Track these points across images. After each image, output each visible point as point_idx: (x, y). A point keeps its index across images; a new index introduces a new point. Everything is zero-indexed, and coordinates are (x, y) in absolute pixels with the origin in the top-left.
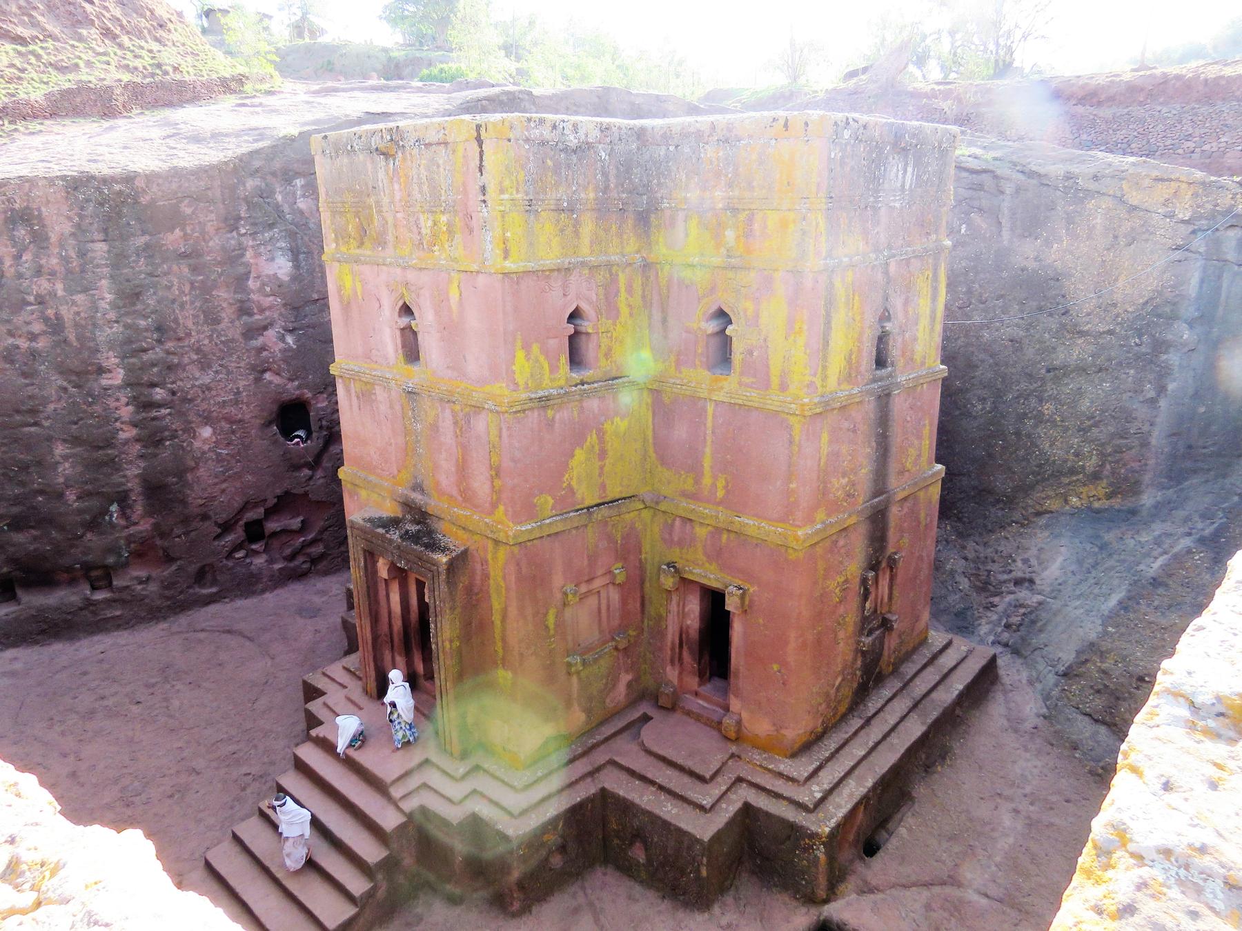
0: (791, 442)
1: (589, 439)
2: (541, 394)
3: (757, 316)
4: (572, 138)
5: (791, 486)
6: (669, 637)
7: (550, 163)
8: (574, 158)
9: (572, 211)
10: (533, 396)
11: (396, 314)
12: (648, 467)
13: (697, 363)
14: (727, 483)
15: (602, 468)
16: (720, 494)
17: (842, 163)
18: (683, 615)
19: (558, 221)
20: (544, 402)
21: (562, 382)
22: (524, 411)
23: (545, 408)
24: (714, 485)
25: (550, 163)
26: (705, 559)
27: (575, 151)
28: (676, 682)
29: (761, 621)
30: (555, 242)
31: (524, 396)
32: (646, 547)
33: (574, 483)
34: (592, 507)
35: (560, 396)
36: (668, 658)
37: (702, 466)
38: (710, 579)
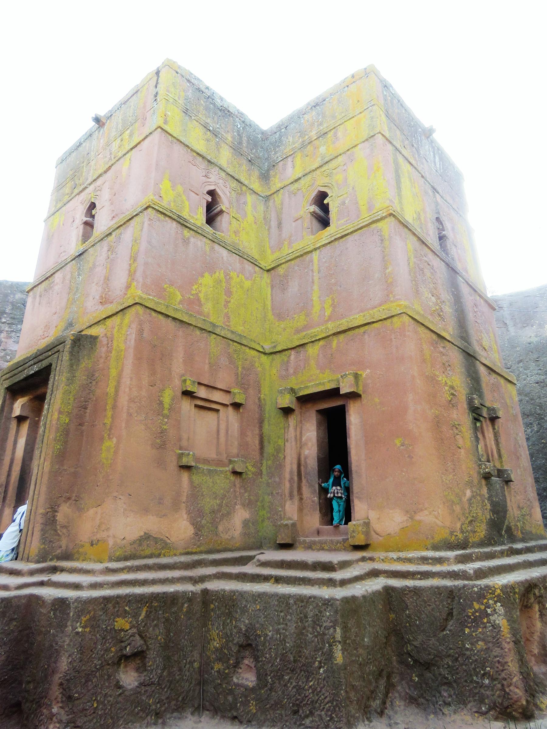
0: (382, 240)
1: (217, 274)
3: (346, 179)
5: (388, 271)
6: (288, 469)
11: (84, 215)
12: (267, 327)
13: (304, 233)
14: (333, 300)
15: (228, 302)
16: (328, 313)
18: (301, 446)
24: (323, 309)
26: (318, 371)
28: (295, 518)
29: (377, 400)
32: (265, 391)
33: (201, 295)
36: (287, 492)
37: (312, 300)
38: (323, 384)
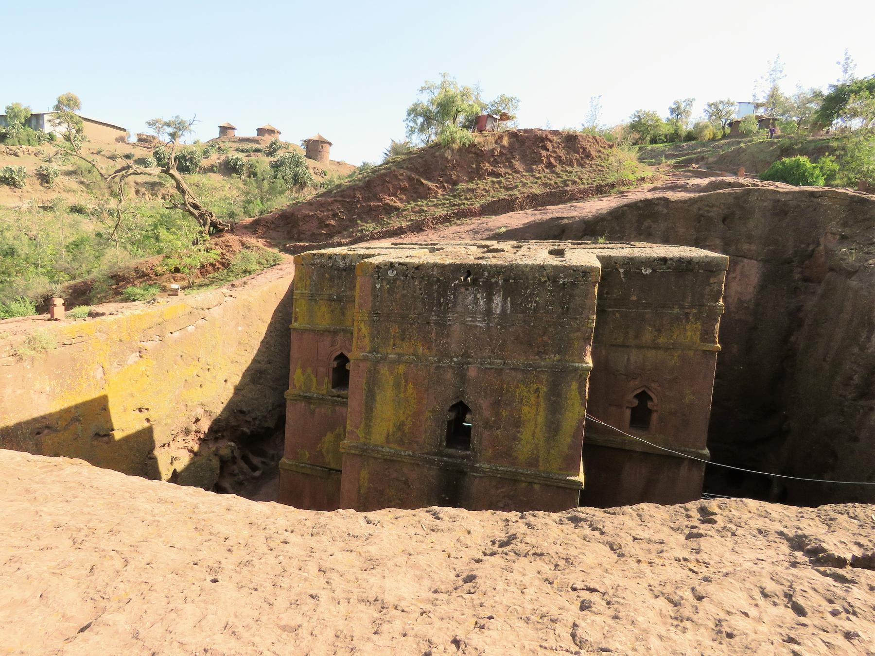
1: (337, 430)
2: (308, 394)
4: (341, 263)
7: (327, 275)
8: (344, 273)
9: (341, 301)
10: (301, 394)
17: (391, 291)
19: (330, 306)
20: (308, 399)
21: (325, 392)
22: (296, 400)
23: (310, 403)
25: (327, 275)
27: (345, 270)
30: (327, 316)
31: (296, 392)
33: (324, 451)
34: (333, 470)
35: (318, 399)
